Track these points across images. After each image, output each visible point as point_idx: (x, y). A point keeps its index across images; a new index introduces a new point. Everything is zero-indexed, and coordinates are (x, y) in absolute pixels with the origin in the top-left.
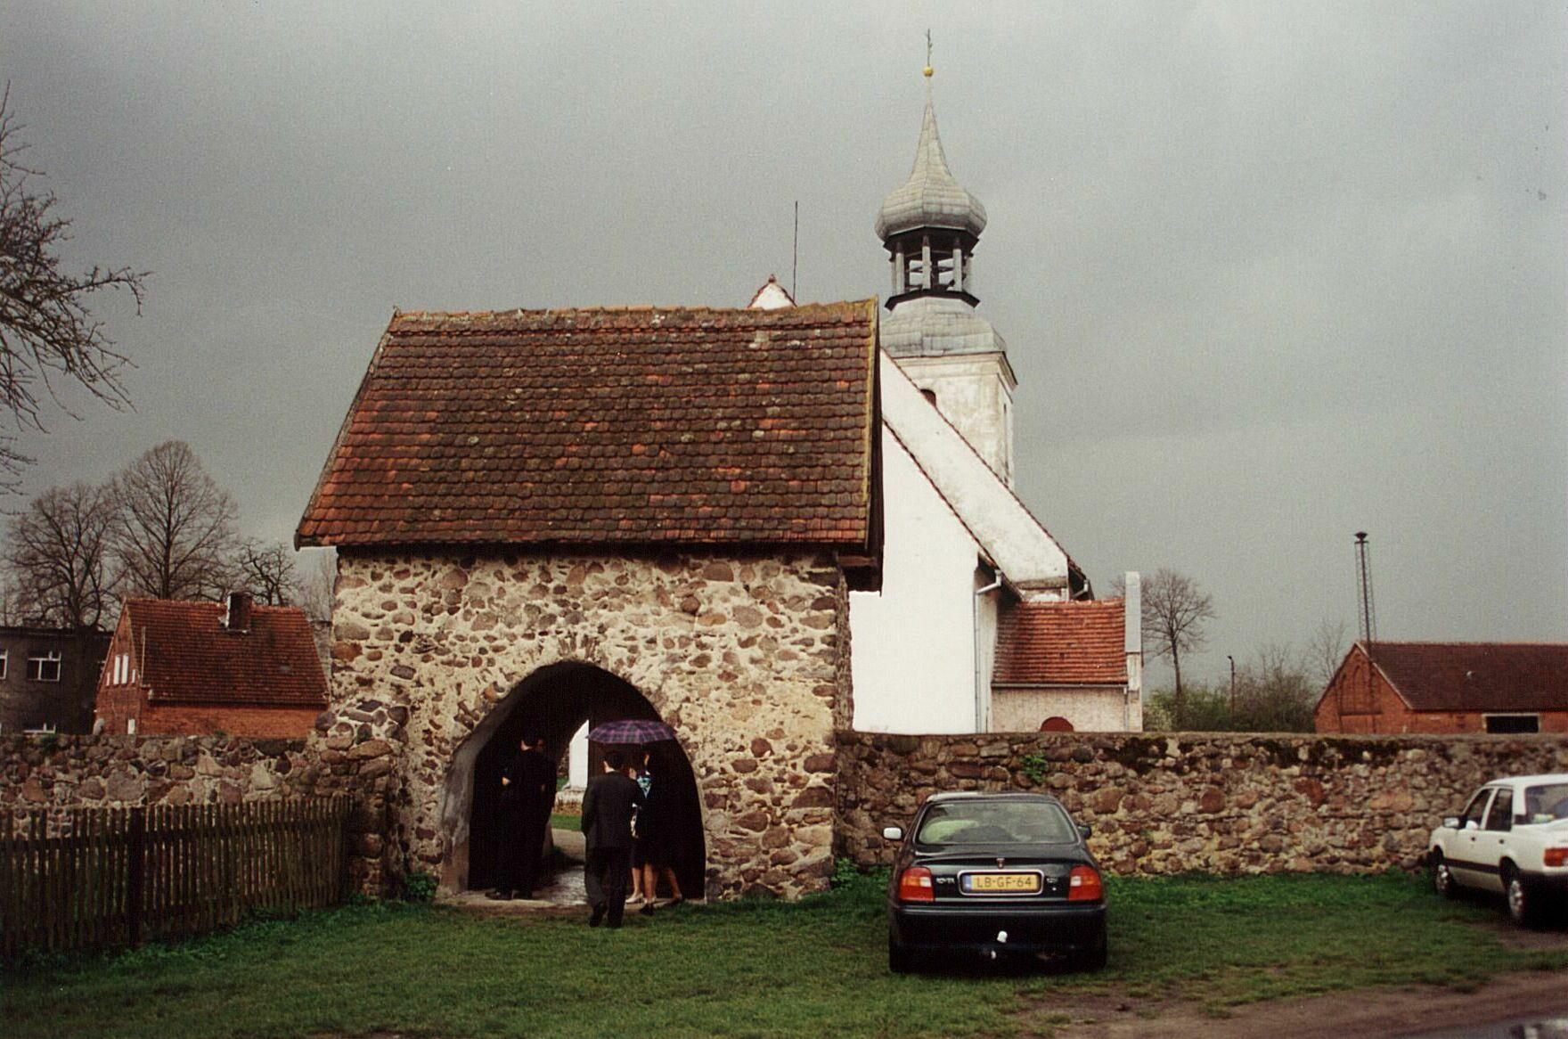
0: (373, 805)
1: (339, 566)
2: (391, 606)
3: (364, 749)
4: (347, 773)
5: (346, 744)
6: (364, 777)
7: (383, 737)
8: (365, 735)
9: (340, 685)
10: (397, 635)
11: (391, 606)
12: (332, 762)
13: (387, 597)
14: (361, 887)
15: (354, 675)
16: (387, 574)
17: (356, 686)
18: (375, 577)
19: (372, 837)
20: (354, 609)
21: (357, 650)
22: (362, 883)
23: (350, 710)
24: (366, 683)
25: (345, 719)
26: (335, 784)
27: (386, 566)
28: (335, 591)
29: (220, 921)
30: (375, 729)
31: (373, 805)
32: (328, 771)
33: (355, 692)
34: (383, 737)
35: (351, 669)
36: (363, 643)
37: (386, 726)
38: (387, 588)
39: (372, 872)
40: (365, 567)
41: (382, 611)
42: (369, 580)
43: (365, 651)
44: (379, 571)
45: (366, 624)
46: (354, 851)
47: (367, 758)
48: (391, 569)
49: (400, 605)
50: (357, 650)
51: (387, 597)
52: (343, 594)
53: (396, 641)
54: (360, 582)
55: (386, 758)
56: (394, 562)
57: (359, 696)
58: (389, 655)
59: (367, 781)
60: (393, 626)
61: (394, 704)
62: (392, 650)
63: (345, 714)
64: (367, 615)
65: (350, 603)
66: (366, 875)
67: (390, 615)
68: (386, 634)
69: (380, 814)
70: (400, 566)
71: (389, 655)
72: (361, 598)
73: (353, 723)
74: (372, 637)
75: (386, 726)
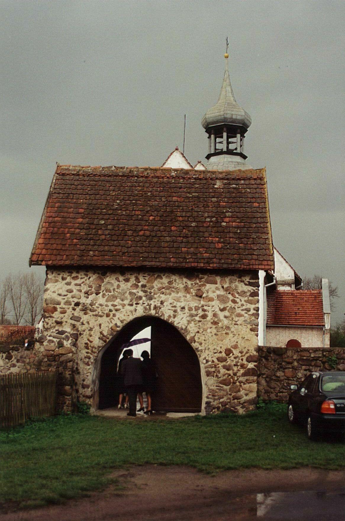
0: (67, 374)
1: (47, 274)
2: (71, 291)
3: (61, 351)
4: (55, 361)
5: (53, 349)
6: (62, 362)
7: (69, 346)
8: (60, 345)
9: (48, 324)
10: (73, 304)
11: (71, 291)
12: (48, 356)
13: (69, 287)
14: (63, 408)
15: (54, 320)
16: (69, 278)
17: (55, 324)
18: (63, 279)
19: (67, 388)
20: (54, 292)
21: (55, 309)
22: (63, 407)
23: (52, 334)
24: (59, 323)
25: (51, 338)
26: (50, 365)
27: (68, 274)
28: (45, 284)
29: (20, 422)
30: (65, 343)
31: (67, 374)
32: (46, 360)
33: (55, 327)
34: (69, 346)
35: (53, 317)
36: (58, 306)
37: (70, 341)
38: (69, 284)
39: (67, 402)
40: (59, 274)
41: (66, 293)
42: (60, 280)
43: (59, 310)
44: (65, 276)
45: (59, 298)
47: (62, 354)
48: (71, 275)
49: (75, 291)
50: (55, 309)
51: (69, 287)
52: (48, 286)
53: (73, 305)
54: (57, 281)
55: (71, 355)
56: (72, 273)
57: (57, 328)
58: (69, 312)
59: (64, 364)
60: (71, 300)
61: (72, 332)
62: (71, 309)
63: (50, 336)
64: (60, 295)
65: (52, 289)
66: (65, 403)
67: (70, 295)
68: (68, 303)
69: (71, 378)
70: (74, 275)
71: (69, 312)
72: (57, 287)
73: (55, 340)
74: (62, 303)
75: (70, 341)
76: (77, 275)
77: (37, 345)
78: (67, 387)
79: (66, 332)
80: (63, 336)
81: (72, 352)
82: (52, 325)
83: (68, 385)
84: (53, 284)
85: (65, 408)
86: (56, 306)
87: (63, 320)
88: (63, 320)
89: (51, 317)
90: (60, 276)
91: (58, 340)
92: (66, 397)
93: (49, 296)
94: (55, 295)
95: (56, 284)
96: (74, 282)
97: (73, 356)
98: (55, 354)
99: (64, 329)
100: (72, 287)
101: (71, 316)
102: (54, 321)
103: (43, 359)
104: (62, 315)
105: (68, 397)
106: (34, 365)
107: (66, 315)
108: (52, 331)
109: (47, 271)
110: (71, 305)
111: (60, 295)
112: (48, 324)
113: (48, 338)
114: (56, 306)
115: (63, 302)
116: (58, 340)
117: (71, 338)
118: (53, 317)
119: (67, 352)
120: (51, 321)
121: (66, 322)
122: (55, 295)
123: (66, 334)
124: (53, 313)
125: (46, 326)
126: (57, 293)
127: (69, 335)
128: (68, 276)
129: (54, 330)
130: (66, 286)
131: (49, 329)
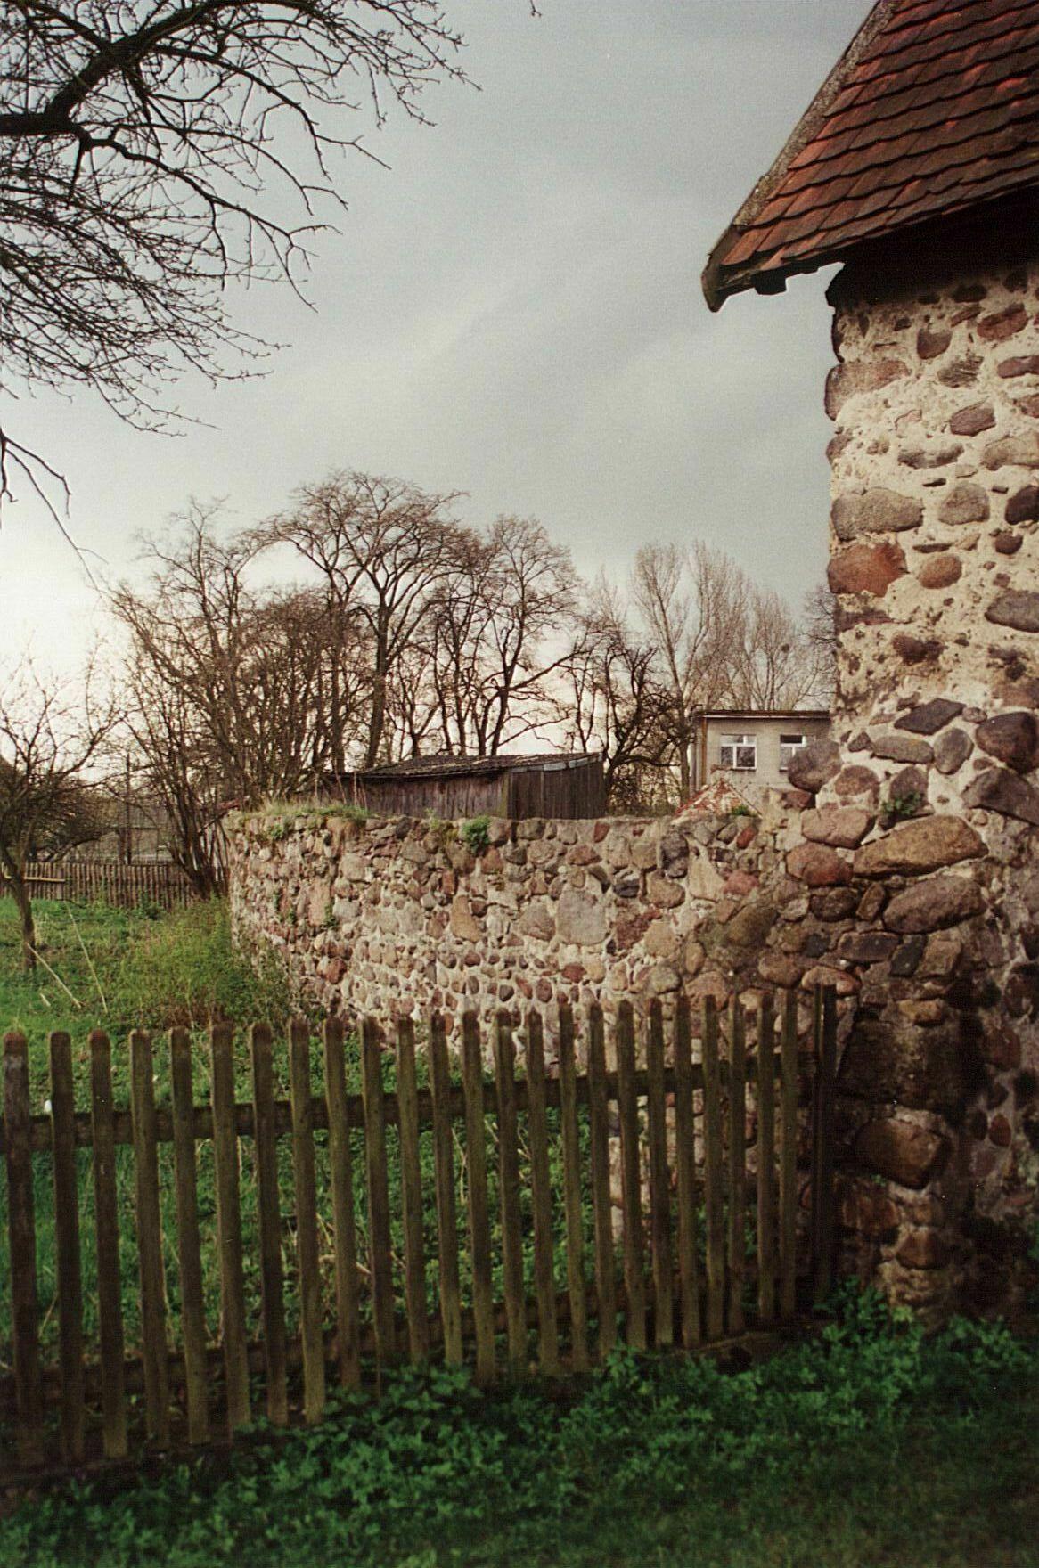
0: (910, 1021)
1: (837, 340)
2: (976, 422)
3: (902, 845)
4: (851, 913)
5: (851, 830)
6: (896, 928)
7: (956, 808)
8: (906, 805)
9: (854, 665)
10: (998, 506)
11: (976, 422)
12: (812, 881)
13: (966, 396)
14: (874, 1272)
15: (889, 632)
16: (961, 331)
17: (894, 664)
18: (928, 347)
19: (908, 1120)
20: (879, 448)
21: (892, 562)
22: (879, 1259)
23: (875, 733)
24: (920, 653)
25: (861, 759)
26: (811, 948)
27: (953, 309)
28: (831, 413)
29: (243, 1421)
30: (936, 786)
31: (910, 1021)
32: (801, 906)
33: (894, 683)
34: (956, 808)
35: (884, 618)
36: (906, 540)
37: (967, 774)
38: (962, 374)
39: (905, 1230)
40: (902, 325)
41: (950, 441)
42: (911, 359)
43: (914, 561)
44: (937, 328)
45: (910, 485)
46: (844, 1150)
47: (911, 871)
48: (971, 315)
49: (1001, 412)
50: (892, 562)
51: (966, 396)
52: (851, 408)
53: (997, 520)
54: (889, 371)
55: (964, 872)
56: (980, 294)
57: (904, 692)
58: (979, 565)
59: (902, 944)
60: (985, 479)
61: (998, 707)
62: (986, 550)
63: (863, 743)
64: (911, 460)
65: (868, 432)
66: (890, 1236)
67: (974, 448)
68: (967, 506)
69: (931, 1047)
70: (992, 305)
71: (979, 565)
72: (891, 414)
73: (878, 767)
74: (930, 517)
75: (967, 774)
76: (1016, 297)
77: (265, 853)
78: (906, 1116)
79: (959, 710)
80: (931, 740)
81: (978, 852)
82: (879, 671)
83: (916, 1105)
84: (868, 395)
85: (888, 1269)
86: (891, 538)
87: (938, 629)
88: (938, 629)
89: (871, 616)
90: (909, 338)
91: (895, 769)
92: (896, 1191)
93: (851, 482)
94: (888, 462)
95: (886, 392)
96: (992, 355)
97: (981, 880)
98: (860, 868)
99: (947, 695)
100: (989, 390)
101: (990, 592)
102: (886, 647)
103: (784, 901)
104: (935, 597)
105: (909, 1195)
106: (728, 942)
107: (957, 591)
108: (876, 709)
109: (835, 319)
110: (984, 517)
111: (911, 460)
112: (854, 665)
113: (849, 759)
114: (891, 538)
115: (931, 501)
116: (895, 769)
117: (978, 754)
118: (884, 618)
119: (938, 853)
120: (868, 644)
121: (962, 642)
122: (888, 462)
123: (957, 723)
124: (880, 594)
125: (848, 683)
126: (894, 452)
127: (970, 729)
128: (956, 322)
129: (890, 705)
130: (942, 389)
131: (862, 698)
